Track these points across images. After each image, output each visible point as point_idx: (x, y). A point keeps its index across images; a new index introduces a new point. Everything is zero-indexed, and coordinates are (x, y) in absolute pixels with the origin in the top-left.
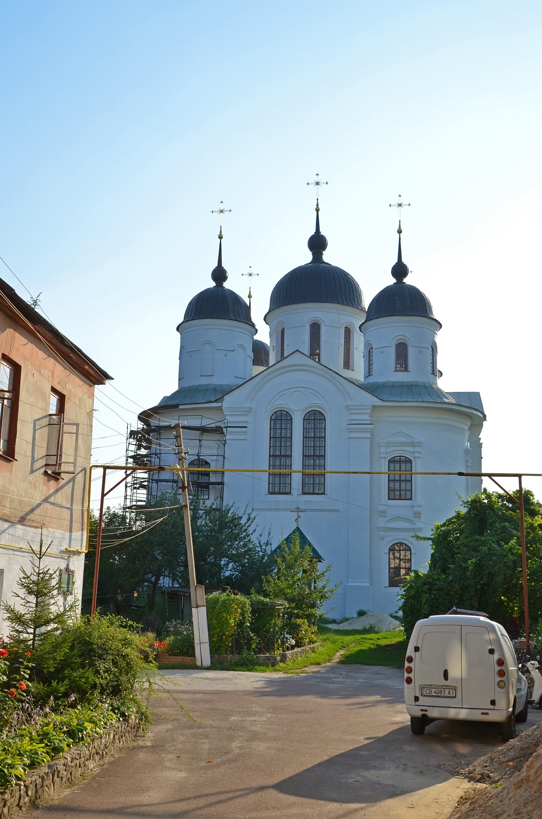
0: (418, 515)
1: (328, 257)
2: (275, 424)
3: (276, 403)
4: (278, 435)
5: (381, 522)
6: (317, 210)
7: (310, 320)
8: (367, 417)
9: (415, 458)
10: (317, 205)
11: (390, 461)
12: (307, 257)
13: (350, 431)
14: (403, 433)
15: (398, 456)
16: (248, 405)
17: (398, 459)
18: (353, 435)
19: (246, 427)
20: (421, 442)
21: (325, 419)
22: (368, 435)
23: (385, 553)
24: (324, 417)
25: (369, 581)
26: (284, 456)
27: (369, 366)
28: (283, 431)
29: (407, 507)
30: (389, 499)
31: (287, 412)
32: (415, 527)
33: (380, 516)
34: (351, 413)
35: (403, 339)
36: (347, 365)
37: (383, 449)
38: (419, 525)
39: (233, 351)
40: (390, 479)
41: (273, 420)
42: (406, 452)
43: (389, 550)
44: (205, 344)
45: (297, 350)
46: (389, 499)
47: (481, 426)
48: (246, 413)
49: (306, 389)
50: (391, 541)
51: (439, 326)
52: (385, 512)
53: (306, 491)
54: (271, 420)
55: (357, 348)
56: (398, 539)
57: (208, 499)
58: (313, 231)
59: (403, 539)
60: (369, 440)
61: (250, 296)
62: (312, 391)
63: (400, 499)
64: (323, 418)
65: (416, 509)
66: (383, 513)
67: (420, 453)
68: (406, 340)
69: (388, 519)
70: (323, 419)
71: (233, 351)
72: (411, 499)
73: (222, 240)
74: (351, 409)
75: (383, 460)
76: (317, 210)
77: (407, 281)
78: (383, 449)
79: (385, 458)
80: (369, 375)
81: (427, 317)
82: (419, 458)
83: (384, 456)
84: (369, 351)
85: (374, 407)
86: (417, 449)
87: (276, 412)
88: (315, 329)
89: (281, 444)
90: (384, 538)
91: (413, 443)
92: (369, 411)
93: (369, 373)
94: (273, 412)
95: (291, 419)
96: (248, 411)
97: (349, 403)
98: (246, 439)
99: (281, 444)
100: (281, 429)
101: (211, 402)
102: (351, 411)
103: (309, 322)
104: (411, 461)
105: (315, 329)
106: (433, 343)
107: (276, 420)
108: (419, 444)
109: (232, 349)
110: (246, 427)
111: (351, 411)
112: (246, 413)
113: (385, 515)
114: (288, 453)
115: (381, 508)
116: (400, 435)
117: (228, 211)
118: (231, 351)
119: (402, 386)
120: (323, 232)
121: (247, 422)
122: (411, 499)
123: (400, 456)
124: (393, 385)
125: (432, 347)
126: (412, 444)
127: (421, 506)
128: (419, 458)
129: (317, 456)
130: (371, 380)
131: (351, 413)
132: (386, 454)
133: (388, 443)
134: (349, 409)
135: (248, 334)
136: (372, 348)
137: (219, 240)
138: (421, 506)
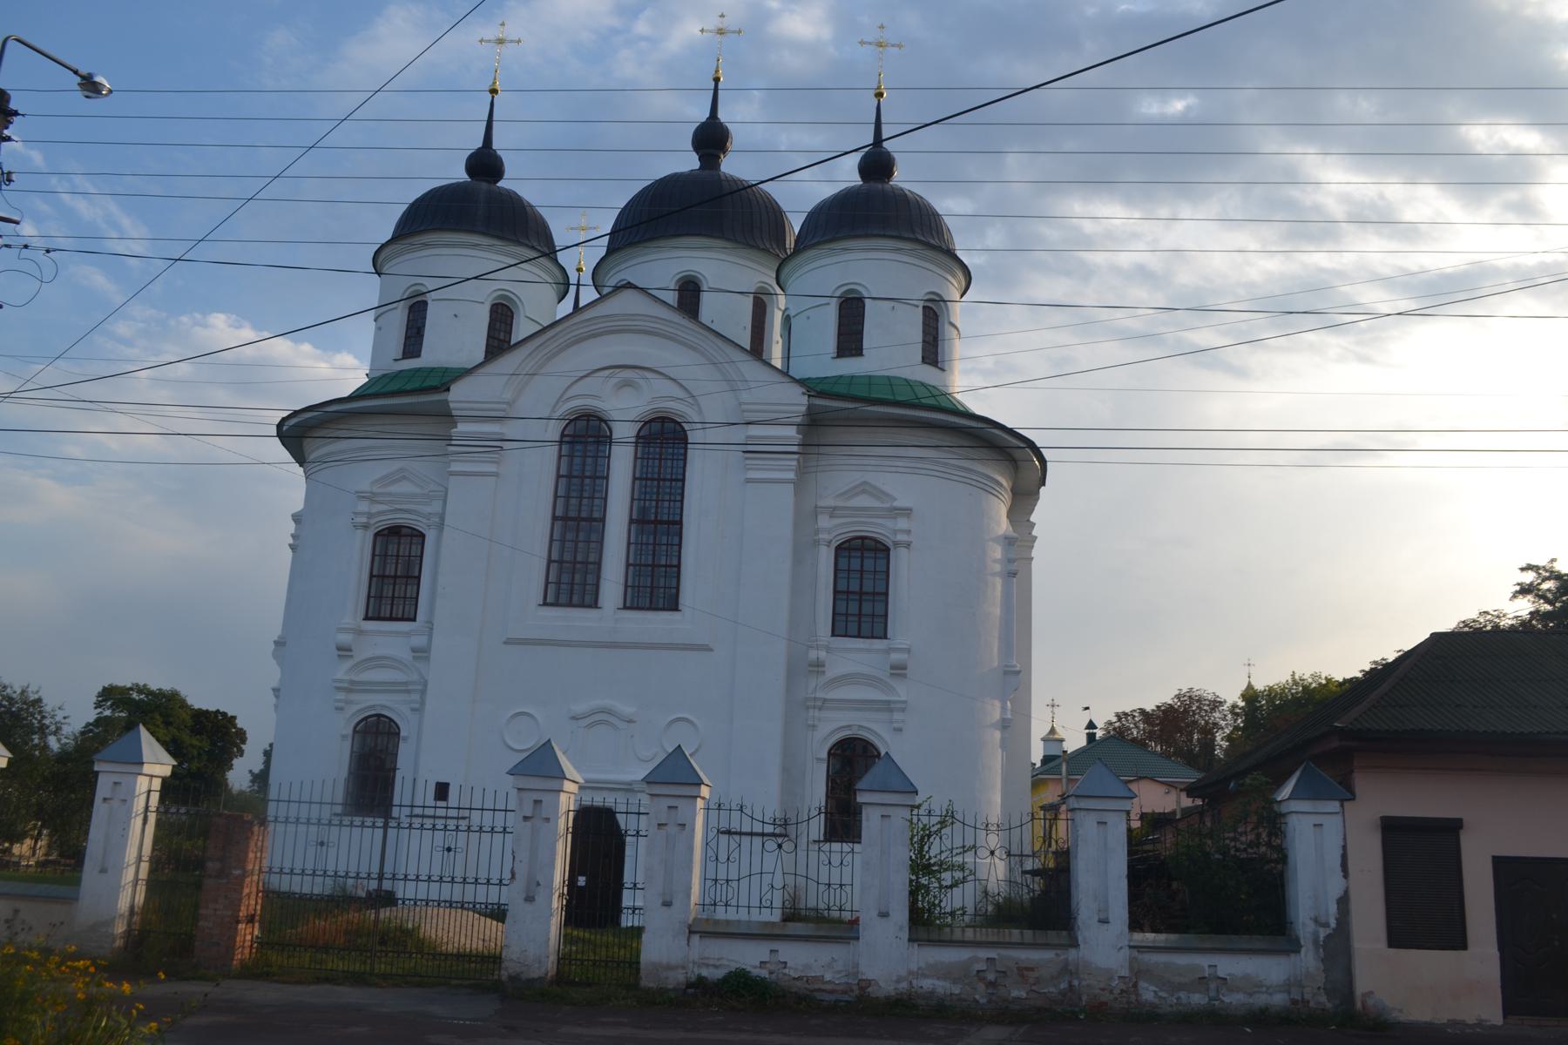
0: (899, 670)
11: (838, 548)
20: (911, 510)
23: (818, 759)
30: (833, 634)
37: (824, 522)
40: (839, 589)
42: (880, 529)
43: (829, 753)
46: (833, 634)
56: (849, 727)
57: (414, 620)
63: (859, 636)
65: (895, 657)
66: (818, 666)
67: (908, 532)
72: (885, 637)
78: (824, 522)
82: (908, 545)
86: (902, 523)
104: (887, 550)
105: (689, 294)
108: (906, 512)
113: (820, 669)
122: (885, 637)
128: (908, 545)
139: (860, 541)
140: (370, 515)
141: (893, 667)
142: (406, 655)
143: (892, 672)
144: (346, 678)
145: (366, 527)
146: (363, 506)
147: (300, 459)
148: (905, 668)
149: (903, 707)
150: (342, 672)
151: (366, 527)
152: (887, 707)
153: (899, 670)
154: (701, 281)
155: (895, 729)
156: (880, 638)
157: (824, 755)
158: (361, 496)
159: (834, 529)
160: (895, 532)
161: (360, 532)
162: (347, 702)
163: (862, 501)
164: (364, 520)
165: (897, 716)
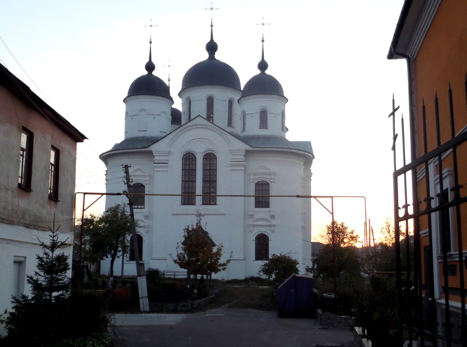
1: (218, 56)
2: (186, 161)
3: (187, 148)
4: (187, 168)
5: (250, 222)
6: (212, 26)
7: (207, 96)
8: (242, 157)
9: (271, 182)
10: (212, 22)
12: (205, 56)
14: (264, 167)
15: (261, 181)
16: (168, 149)
17: (261, 183)
18: (233, 168)
19: (167, 163)
21: (216, 158)
22: (243, 168)
23: (253, 240)
24: (216, 157)
25: (243, 257)
26: (190, 181)
27: (244, 126)
28: (190, 166)
29: (267, 212)
30: (256, 207)
31: (193, 154)
32: (271, 224)
33: (250, 217)
34: (233, 155)
35: (264, 108)
36: (230, 124)
37: (252, 177)
38: (273, 222)
39: (159, 115)
41: (184, 159)
42: (266, 178)
44: (142, 110)
45: (199, 115)
46: (256, 207)
47: (312, 162)
48: (168, 154)
49: (205, 140)
50: (256, 233)
51: (286, 101)
52: (252, 215)
53: (205, 203)
54: (183, 159)
55: (236, 114)
57: (144, 208)
58: (209, 40)
59: (264, 231)
60: (243, 172)
61: (169, 80)
62: (208, 141)
64: (215, 158)
65: (272, 213)
66: (252, 216)
67: (274, 179)
68: (266, 110)
69: (254, 219)
70: (215, 158)
71: (159, 115)
74: (232, 152)
75: (252, 183)
76: (212, 26)
77: (267, 72)
78: (252, 177)
79: (253, 182)
80: (244, 131)
81: (279, 95)
82: (274, 182)
83: (253, 181)
84: (244, 115)
85: (247, 152)
86: (273, 177)
87: (186, 154)
88: (210, 101)
89: (189, 174)
90: (252, 231)
91: (270, 173)
92: (244, 153)
93: (244, 130)
94: (184, 154)
95: (195, 158)
96: (169, 154)
98: (167, 171)
99: (189, 174)
100: (189, 164)
101: (145, 147)
102: (233, 153)
103: (206, 97)
104: (269, 184)
105: (210, 101)
106: (283, 111)
107: (185, 159)
108: (274, 174)
109: (158, 114)
110: (167, 163)
111: (233, 153)
112: (168, 154)
113: (252, 217)
114: (194, 179)
115: (251, 213)
116: (262, 168)
117: (155, 26)
118: (158, 115)
119: (264, 138)
120: (215, 40)
121: (168, 160)
122: (269, 207)
123: (262, 181)
124: (258, 137)
125: (282, 113)
126: (270, 174)
127: (275, 212)
128: (274, 182)
129: (211, 181)
130: (245, 134)
131: (233, 155)
132: (254, 179)
133: (255, 173)
134: (231, 152)
135: (168, 104)
136: (245, 114)
138: (275, 212)
139: (261, 182)
141: (271, 216)
142: (143, 218)
143: (271, 217)
147: (106, 163)
148: (274, 216)
149: (274, 226)
152: (270, 226)
153: (273, 217)
154: (212, 96)
155: (272, 231)
156: (267, 207)
157: (254, 239)
159: (255, 179)
160: (270, 179)
163: (263, 171)
165: (273, 228)
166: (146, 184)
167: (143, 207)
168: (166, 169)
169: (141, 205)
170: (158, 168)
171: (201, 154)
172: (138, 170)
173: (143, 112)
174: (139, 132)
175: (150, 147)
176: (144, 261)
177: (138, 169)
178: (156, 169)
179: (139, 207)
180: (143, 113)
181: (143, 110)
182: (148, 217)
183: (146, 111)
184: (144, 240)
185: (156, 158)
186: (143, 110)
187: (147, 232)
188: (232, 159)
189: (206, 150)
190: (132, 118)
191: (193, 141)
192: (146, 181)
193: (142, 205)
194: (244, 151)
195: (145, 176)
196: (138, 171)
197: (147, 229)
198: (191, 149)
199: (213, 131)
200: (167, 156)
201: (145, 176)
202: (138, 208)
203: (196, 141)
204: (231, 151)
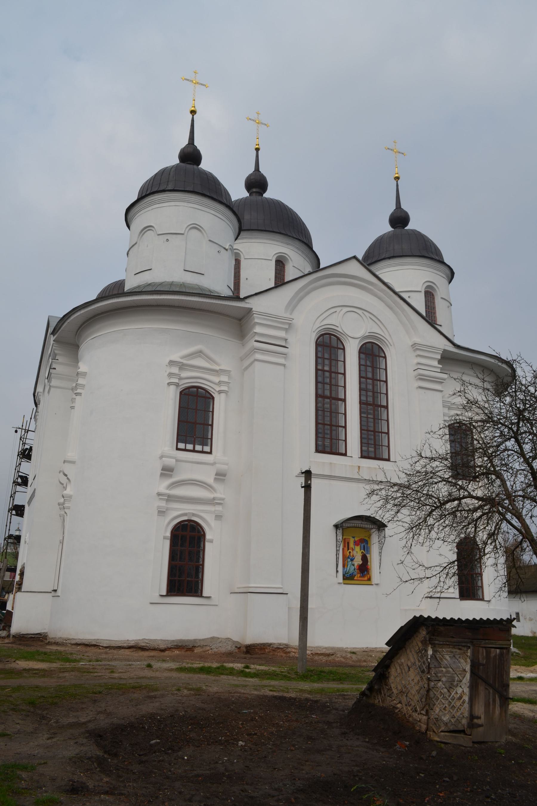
3: (325, 322)
6: (257, 150)
8: (436, 363)
13: (422, 378)
16: (287, 315)
31: (338, 339)
57: (211, 453)
68: (435, 290)
73: (195, 116)
76: (257, 150)
87: (322, 335)
97: (418, 340)
98: (284, 365)
111: (419, 353)
112: (287, 327)
121: (286, 340)
137: (190, 116)
140: (180, 379)
142: (210, 480)
144: (168, 492)
145: (177, 385)
146: (175, 370)
150: (163, 486)
151: (177, 385)
158: (172, 363)
161: (173, 387)
162: (167, 509)
164: (176, 381)
166: (220, 392)
167: (207, 449)
168: (282, 361)
169: (203, 444)
170: (263, 354)
171: (358, 340)
172: (199, 354)
173: (194, 231)
174: (185, 272)
175: (247, 301)
176: (209, 598)
177: (201, 352)
178: (258, 356)
179: (198, 448)
180: (194, 232)
181: (196, 227)
182: (224, 475)
183: (203, 231)
184: (208, 537)
185: (258, 329)
186: (196, 227)
187: (218, 517)
188: (419, 364)
189: (367, 334)
190: (167, 240)
191: (339, 309)
192: (220, 383)
193: (207, 445)
194: (441, 352)
195: (217, 372)
196: (200, 356)
197: (219, 508)
198: (338, 327)
199: (380, 298)
200: (286, 330)
201: (217, 372)
202: (194, 451)
203: (345, 309)
204: (415, 347)
